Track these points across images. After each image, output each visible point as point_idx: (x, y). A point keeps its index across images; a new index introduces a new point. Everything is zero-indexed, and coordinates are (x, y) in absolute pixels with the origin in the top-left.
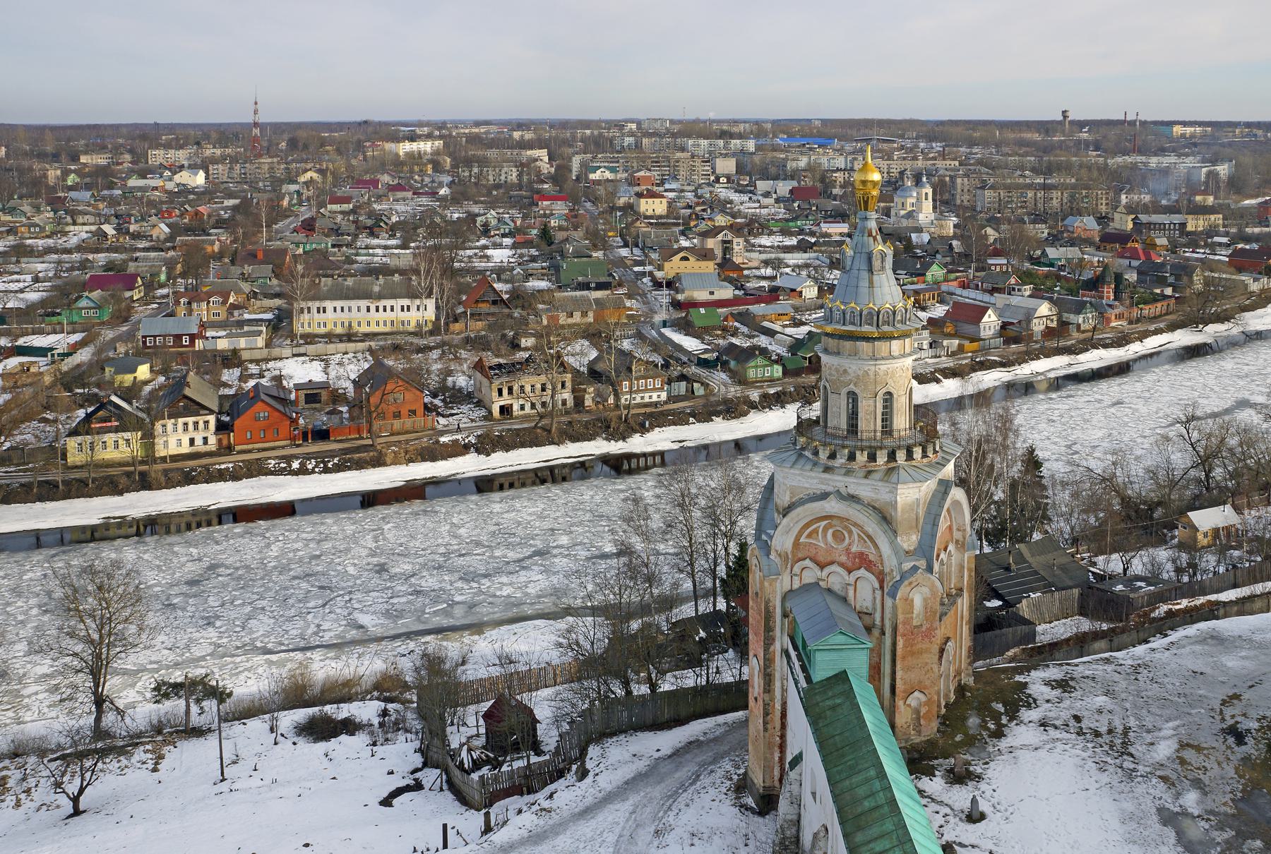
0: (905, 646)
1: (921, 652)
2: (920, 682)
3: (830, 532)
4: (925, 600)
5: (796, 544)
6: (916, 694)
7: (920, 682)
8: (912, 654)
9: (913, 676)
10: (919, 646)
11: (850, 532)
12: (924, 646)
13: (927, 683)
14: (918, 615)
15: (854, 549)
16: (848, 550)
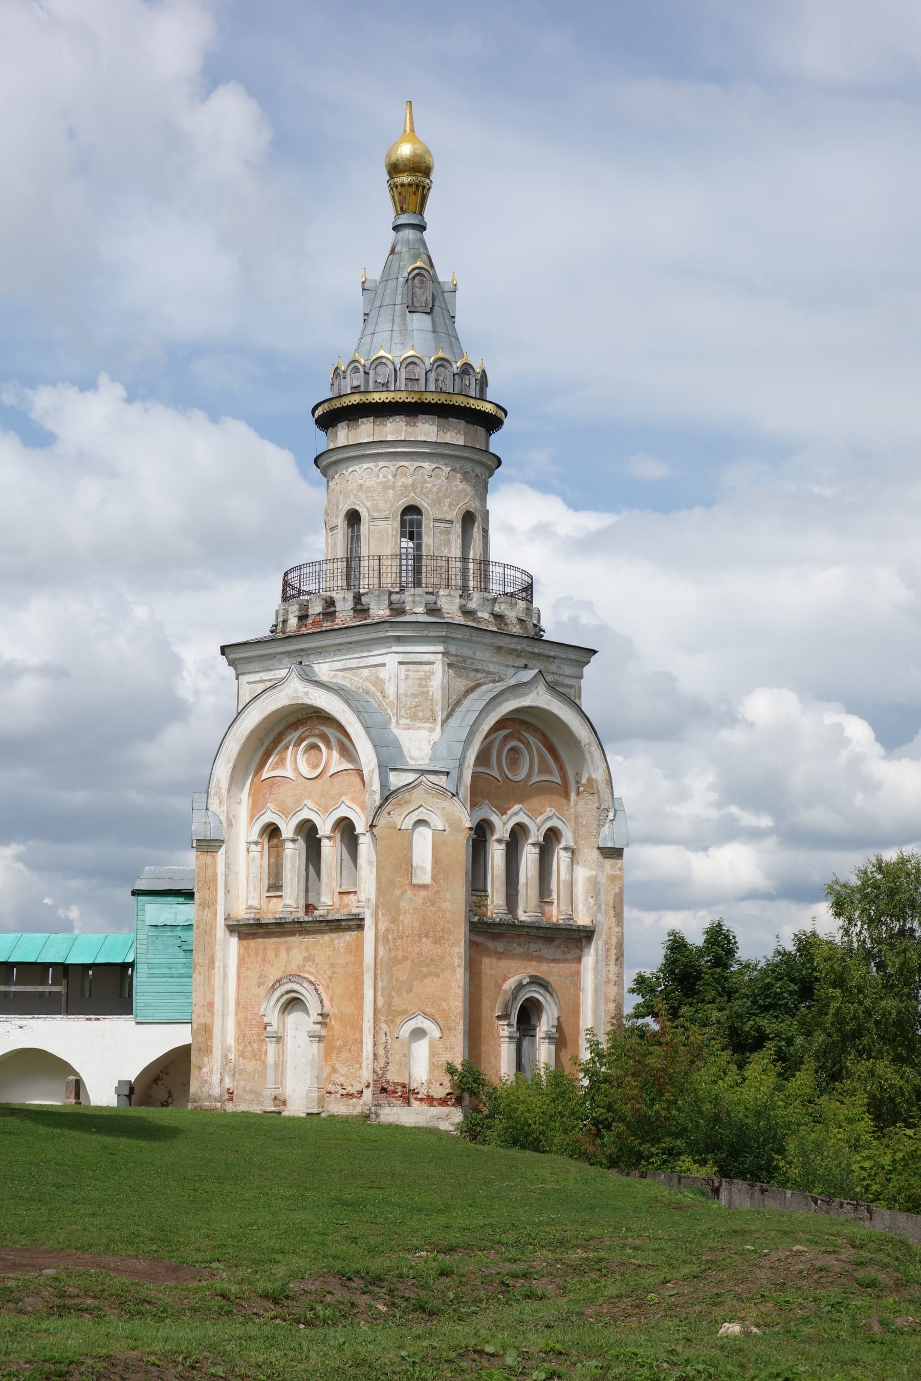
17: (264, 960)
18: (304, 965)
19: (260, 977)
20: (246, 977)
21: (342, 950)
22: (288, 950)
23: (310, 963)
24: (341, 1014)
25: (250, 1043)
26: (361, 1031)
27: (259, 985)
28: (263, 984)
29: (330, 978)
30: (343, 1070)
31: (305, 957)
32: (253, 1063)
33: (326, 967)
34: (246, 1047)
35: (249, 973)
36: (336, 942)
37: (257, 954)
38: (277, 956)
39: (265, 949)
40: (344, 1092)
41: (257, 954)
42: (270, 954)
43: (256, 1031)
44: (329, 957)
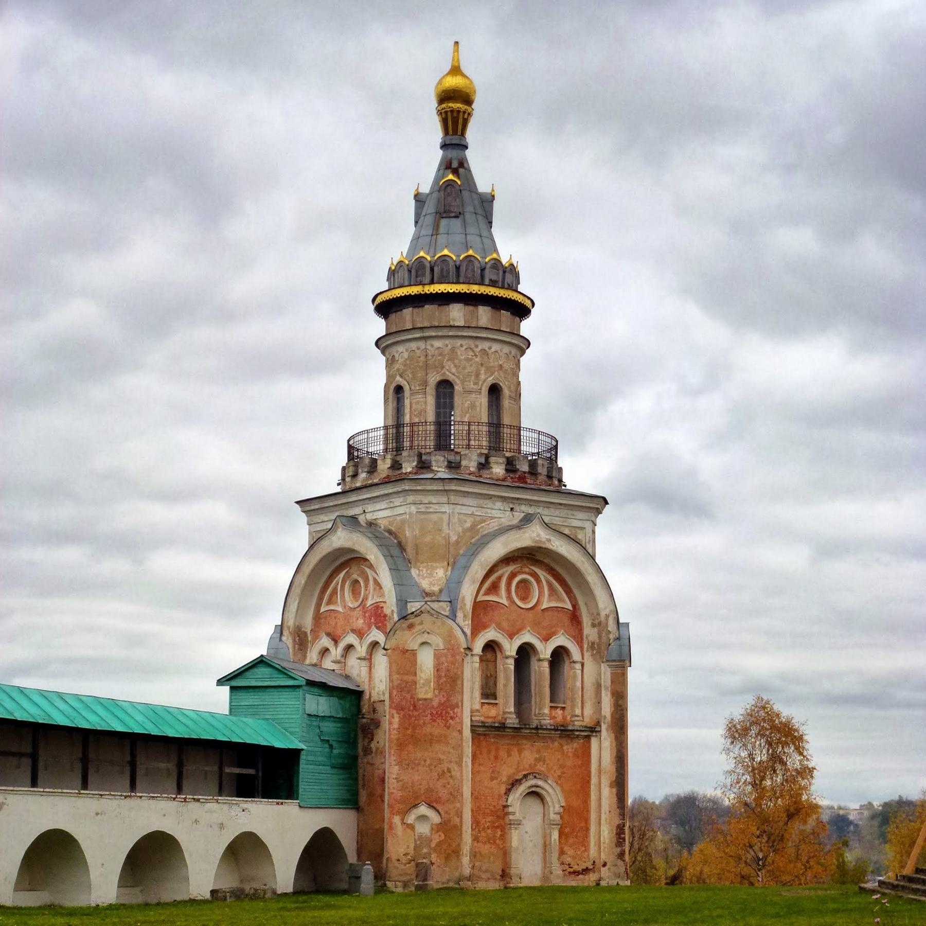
0: (403, 727)
1: (431, 740)
2: (429, 790)
3: (347, 584)
4: (437, 656)
5: (317, 617)
6: (423, 810)
7: (429, 790)
8: (415, 740)
9: (419, 778)
10: (428, 729)
11: (366, 580)
12: (436, 731)
13: (443, 793)
14: (428, 682)
15: (369, 602)
16: (365, 605)
17: (496, 758)
18: (535, 765)
19: (493, 772)
20: (478, 772)
21: (570, 754)
22: (520, 752)
23: (541, 763)
24: (569, 806)
25: (484, 829)
26: (587, 820)
27: (492, 779)
28: (497, 779)
29: (560, 777)
30: (570, 852)
31: (536, 759)
32: (488, 846)
33: (555, 768)
34: (480, 832)
35: (482, 768)
36: (565, 748)
37: (489, 752)
38: (509, 755)
39: (497, 749)
40: (572, 870)
41: (489, 752)
42: (503, 754)
43: (489, 819)
44: (558, 760)
